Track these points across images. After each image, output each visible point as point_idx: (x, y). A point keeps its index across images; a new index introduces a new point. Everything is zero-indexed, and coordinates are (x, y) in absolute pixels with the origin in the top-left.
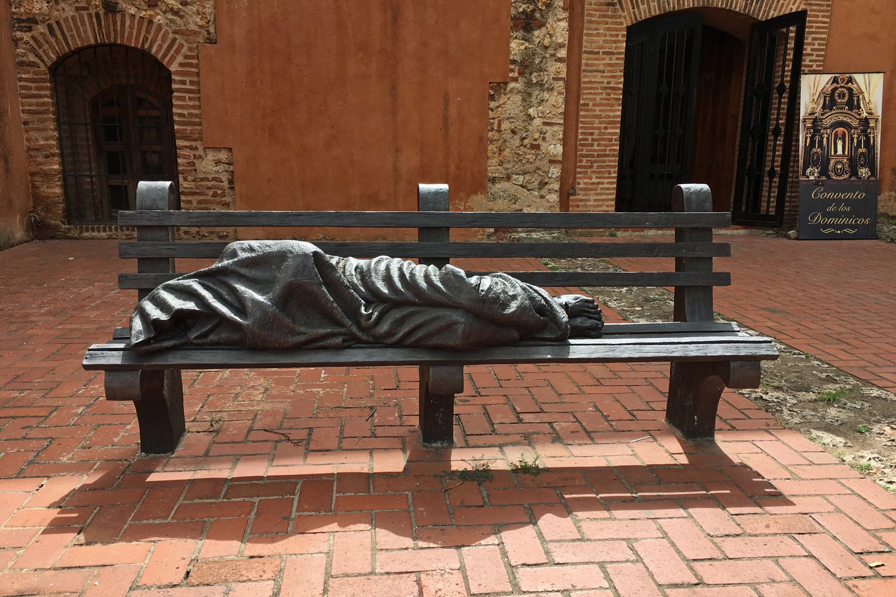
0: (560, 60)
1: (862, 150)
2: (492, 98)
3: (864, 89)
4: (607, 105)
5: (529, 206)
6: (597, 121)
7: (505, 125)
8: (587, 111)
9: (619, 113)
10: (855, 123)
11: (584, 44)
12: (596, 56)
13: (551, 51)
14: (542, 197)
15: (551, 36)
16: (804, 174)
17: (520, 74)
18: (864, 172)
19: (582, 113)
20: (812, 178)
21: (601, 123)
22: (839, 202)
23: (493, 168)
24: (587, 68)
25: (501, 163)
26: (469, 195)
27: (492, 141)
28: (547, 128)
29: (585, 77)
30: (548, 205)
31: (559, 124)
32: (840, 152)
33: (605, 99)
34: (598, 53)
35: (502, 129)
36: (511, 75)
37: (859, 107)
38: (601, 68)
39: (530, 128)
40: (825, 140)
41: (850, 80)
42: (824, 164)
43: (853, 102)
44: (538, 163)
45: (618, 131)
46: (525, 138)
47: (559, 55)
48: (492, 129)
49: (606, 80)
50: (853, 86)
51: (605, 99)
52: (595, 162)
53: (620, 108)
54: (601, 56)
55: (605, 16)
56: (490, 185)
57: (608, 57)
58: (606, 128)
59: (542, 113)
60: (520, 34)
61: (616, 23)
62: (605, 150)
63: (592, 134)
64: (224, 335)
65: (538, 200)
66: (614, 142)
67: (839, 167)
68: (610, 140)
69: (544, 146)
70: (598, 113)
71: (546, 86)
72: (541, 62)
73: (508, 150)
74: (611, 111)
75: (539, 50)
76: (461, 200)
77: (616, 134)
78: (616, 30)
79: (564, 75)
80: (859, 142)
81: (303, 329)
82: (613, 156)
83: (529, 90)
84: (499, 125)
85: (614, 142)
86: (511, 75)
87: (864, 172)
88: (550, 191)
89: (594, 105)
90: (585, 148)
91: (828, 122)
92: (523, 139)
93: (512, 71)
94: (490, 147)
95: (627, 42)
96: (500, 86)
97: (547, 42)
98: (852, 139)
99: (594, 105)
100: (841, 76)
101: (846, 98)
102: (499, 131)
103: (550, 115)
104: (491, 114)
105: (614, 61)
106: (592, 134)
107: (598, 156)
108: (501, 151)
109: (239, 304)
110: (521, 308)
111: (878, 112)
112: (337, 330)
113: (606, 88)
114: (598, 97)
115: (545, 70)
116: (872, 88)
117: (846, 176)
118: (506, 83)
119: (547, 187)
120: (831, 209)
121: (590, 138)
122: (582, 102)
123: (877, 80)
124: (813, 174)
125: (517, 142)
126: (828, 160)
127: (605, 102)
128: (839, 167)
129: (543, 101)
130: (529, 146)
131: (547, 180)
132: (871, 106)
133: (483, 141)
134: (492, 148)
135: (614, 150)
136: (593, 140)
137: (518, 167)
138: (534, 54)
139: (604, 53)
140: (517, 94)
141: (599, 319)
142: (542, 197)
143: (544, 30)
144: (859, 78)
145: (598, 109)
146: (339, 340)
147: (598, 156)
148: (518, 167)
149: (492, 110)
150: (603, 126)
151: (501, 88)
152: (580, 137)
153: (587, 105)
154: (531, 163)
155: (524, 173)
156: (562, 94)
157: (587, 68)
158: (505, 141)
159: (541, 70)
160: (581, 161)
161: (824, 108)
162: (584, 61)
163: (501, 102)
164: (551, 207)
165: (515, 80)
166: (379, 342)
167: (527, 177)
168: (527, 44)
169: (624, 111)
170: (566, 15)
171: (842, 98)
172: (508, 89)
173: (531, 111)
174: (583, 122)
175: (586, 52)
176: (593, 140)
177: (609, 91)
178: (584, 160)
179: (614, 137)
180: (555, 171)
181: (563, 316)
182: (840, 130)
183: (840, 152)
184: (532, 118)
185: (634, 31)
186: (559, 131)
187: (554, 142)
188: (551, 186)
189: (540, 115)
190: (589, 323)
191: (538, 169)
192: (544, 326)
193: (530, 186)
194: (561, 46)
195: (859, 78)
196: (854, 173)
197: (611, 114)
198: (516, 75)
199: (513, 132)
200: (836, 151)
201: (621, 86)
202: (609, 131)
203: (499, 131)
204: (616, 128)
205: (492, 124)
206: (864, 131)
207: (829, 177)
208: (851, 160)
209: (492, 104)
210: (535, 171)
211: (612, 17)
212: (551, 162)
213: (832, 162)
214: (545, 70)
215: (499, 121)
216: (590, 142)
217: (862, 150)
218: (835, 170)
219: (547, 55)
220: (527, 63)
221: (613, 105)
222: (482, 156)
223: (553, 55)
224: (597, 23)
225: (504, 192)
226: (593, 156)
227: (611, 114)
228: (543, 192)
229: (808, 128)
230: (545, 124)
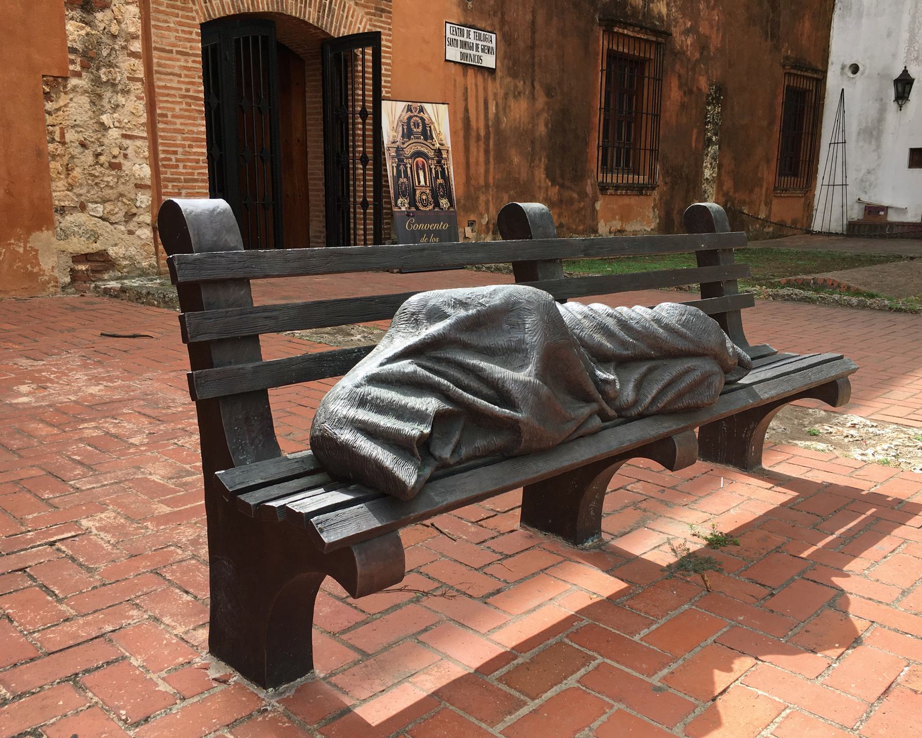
0: (133, 55)
1: (440, 181)
2: (47, 96)
3: (434, 120)
4: (189, 118)
5: (116, 245)
6: (179, 136)
7: (70, 136)
8: (166, 123)
9: (204, 129)
10: (431, 154)
11: (154, 38)
12: (169, 55)
13: (120, 42)
14: (131, 233)
15: (119, 22)
16: (396, 205)
17: (83, 67)
18: (444, 202)
19: (160, 126)
20: (403, 209)
21: (184, 139)
22: (429, 233)
23: (60, 193)
24: (161, 69)
25: (70, 187)
26: (29, 231)
27: (54, 157)
29: (159, 79)
30: (139, 242)
31: (142, 138)
32: (423, 183)
33: (186, 110)
34: (171, 52)
35: (67, 140)
36: (71, 67)
37: (432, 138)
38: (177, 70)
39: (106, 141)
40: (409, 170)
41: (422, 110)
42: (410, 193)
44: (121, 188)
45: (205, 150)
46: (100, 154)
47: (132, 49)
48: (53, 140)
49: (184, 87)
50: (425, 116)
51: (186, 110)
52: (183, 188)
53: (204, 122)
54: (174, 55)
55: (173, 7)
56: (57, 217)
57: (183, 58)
58: (190, 146)
59: (119, 122)
60: (77, 13)
61: (188, 17)
62: (193, 174)
63: (175, 153)
65: (126, 237)
66: (201, 164)
67: (424, 197)
68: (197, 161)
69: (126, 165)
70: (178, 126)
71: (120, 87)
72: (109, 55)
73: (77, 169)
74: (194, 125)
75: (105, 39)
76: (19, 240)
77: (202, 154)
78: (189, 26)
79: (141, 74)
80: (437, 172)
82: (203, 181)
83: (98, 91)
84: (63, 135)
85: (201, 164)
86: (71, 67)
87: (444, 202)
89: (173, 116)
90: (169, 171)
91: (408, 151)
92: (97, 155)
93: (73, 62)
94: (53, 165)
95: (203, 42)
96: (58, 82)
97: (114, 29)
98: (431, 169)
99: (173, 116)
100: (414, 105)
101: (421, 127)
102: (63, 143)
103: (129, 125)
104: (49, 120)
105: (190, 65)
106: (175, 153)
107: (186, 181)
108: (68, 170)
111: (448, 143)
113: (184, 97)
114: (177, 107)
115: (117, 67)
116: (440, 117)
117: (431, 207)
118: (66, 79)
119: (135, 219)
121: (173, 157)
122: (159, 111)
123: (443, 110)
124: (403, 204)
125: (90, 160)
126: (414, 191)
127: (186, 113)
128: (424, 197)
129: (118, 106)
130: (107, 165)
131: (134, 210)
132: (442, 137)
133: (41, 157)
134: (55, 166)
135: (203, 174)
136: (177, 160)
137: (94, 193)
138: (99, 44)
139: (178, 52)
140: (82, 94)
142: (131, 233)
143: (108, 12)
144: (428, 107)
145: (178, 121)
147: (186, 181)
148: (94, 193)
149: (50, 113)
150: (187, 143)
151: (58, 83)
152: (162, 156)
153: (165, 116)
154: (112, 188)
155: (104, 201)
156: (141, 99)
157: (161, 69)
158: (73, 157)
159: (110, 65)
160: (166, 187)
161: (403, 136)
162: (155, 60)
163: (61, 103)
164: (144, 245)
165: (78, 75)
167: (109, 207)
168: (88, 29)
169: (209, 126)
172: (69, 86)
173: (105, 118)
174: (163, 138)
175: (156, 49)
176: (177, 160)
177: (189, 100)
178: (170, 185)
179: (201, 158)
180: (144, 199)
183: (423, 183)
184: (105, 128)
186: (144, 146)
187: (139, 161)
188: (141, 218)
189: (117, 124)
191: (122, 195)
193: (113, 219)
194: (134, 37)
195: (428, 107)
196: (437, 204)
197: (195, 129)
198: (78, 68)
199: (83, 145)
200: (419, 182)
201: (202, 95)
202: (195, 150)
203: (63, 143)
204: (202, 147)
205: (51, 133)
206: (439, 162)
207: (417, 208)
208: (432, 190)
209: (49, 106)
210: (117, 199)
211: (183, 9)
212: (138, 186)
213: (418, 192)
214: (117, 67)
215: (62, 129)
216: (173, 162)
217: (440, 181)
218: (421, 200)
219: (117, 47)
220: (91, 54)
221: (195, 119)
222: (42, 176)
223: (124, 48)
224: (167, 14)
225: (79, 226)
226: (179, 180)
227: (195, 129)
228: (131, 226)
229: (393, 157)
230: (125, 136)
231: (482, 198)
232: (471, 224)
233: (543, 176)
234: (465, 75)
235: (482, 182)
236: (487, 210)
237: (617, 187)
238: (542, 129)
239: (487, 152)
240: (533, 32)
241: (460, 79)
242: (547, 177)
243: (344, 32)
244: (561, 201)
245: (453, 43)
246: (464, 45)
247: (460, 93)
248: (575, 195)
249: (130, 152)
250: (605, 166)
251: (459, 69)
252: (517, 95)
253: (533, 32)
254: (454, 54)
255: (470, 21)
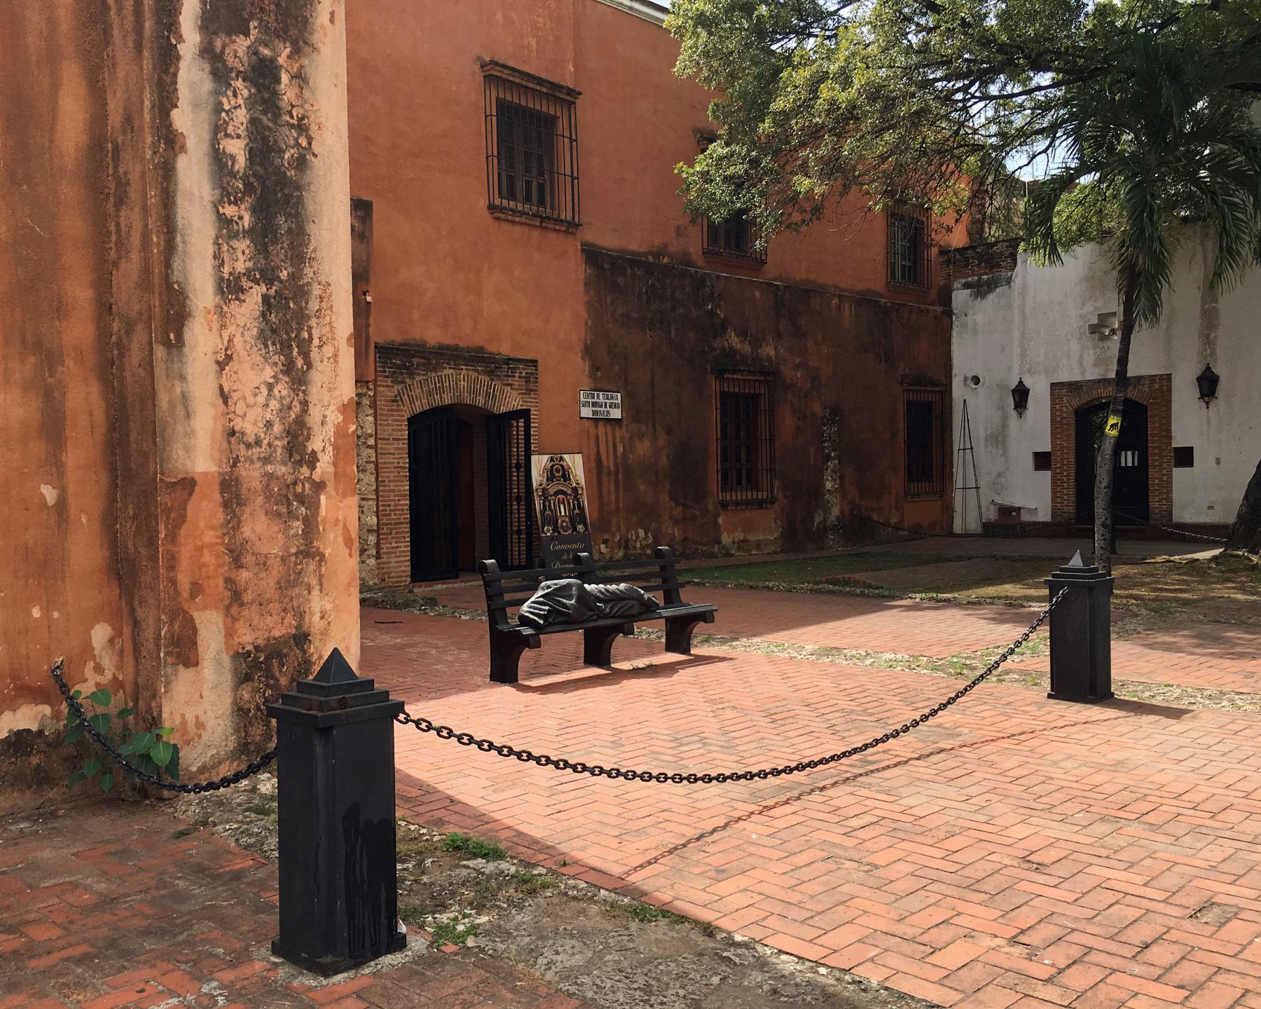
0: (369, 447)
1: (577, 511)
10: (569, 492)
18: (580, 528)
28: (364, 503)
41: (562, 459)
42: (553, 521)
43: (566, 476)
87: (580, 528)
88: (369, 557)
91: (552, 491)
97: (359, 432)
116: (576, 464)
120: (565, 557)
124: (548, 531)
144: (566, 457)
170: (371, 411)
171: (558, 473)
182: (561, 496)
185: (411, 421)
195: (566, 457)
196: (575, 529)
208: (571, 519)
217: (577, 511)
228: (364, 558)
231: (614, 520)
232: (605, 542)
233: (667, 499)
234: (596, 427)
235: (613, 506)
236: (619, 530)
237: (737, 504)
238: (664, 461)
239: (617, 482)
240: (653, 387)
241: (592, 430)
242: (671, 499)
243: (503, 409)
244: (685, 518)
245: (586, 404)
246: (595, 404)
247: (592, 442)
248: (697, 513)
249: (365, 509)
250: (726, 484)
251: (592, 423)
252: (641, 437)
253: (653, 387)
254: (586, 412)
255: (599, 386)
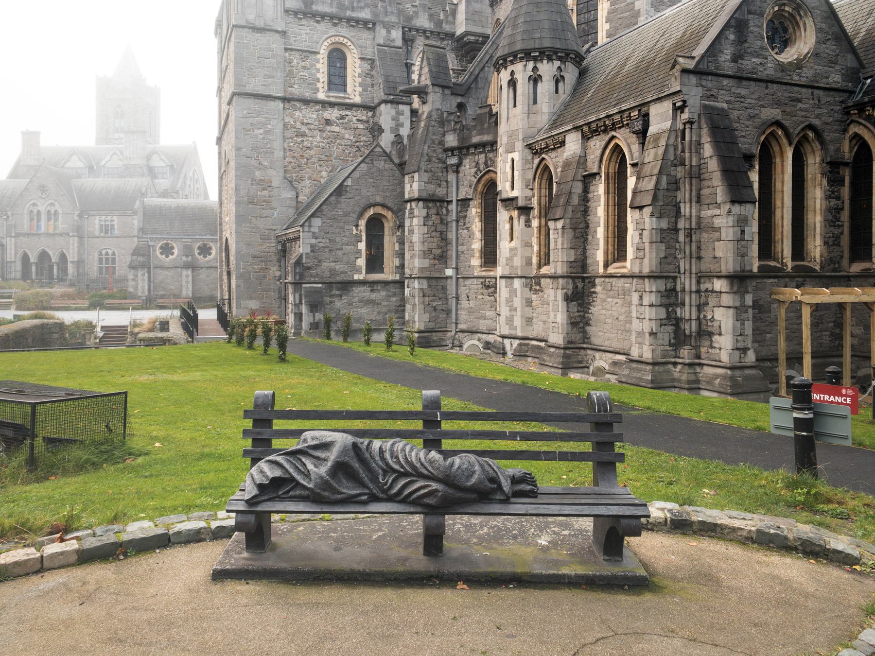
64: (298, 492)
81: (344, 491)
109: (307, 475)
110: (480, 481)
112: (367, 491)
141: (536, 486)
146: (365, 497)
166: (391, 499)
181: (506, 486)
190: (529, 488)
192: (493, 491)
